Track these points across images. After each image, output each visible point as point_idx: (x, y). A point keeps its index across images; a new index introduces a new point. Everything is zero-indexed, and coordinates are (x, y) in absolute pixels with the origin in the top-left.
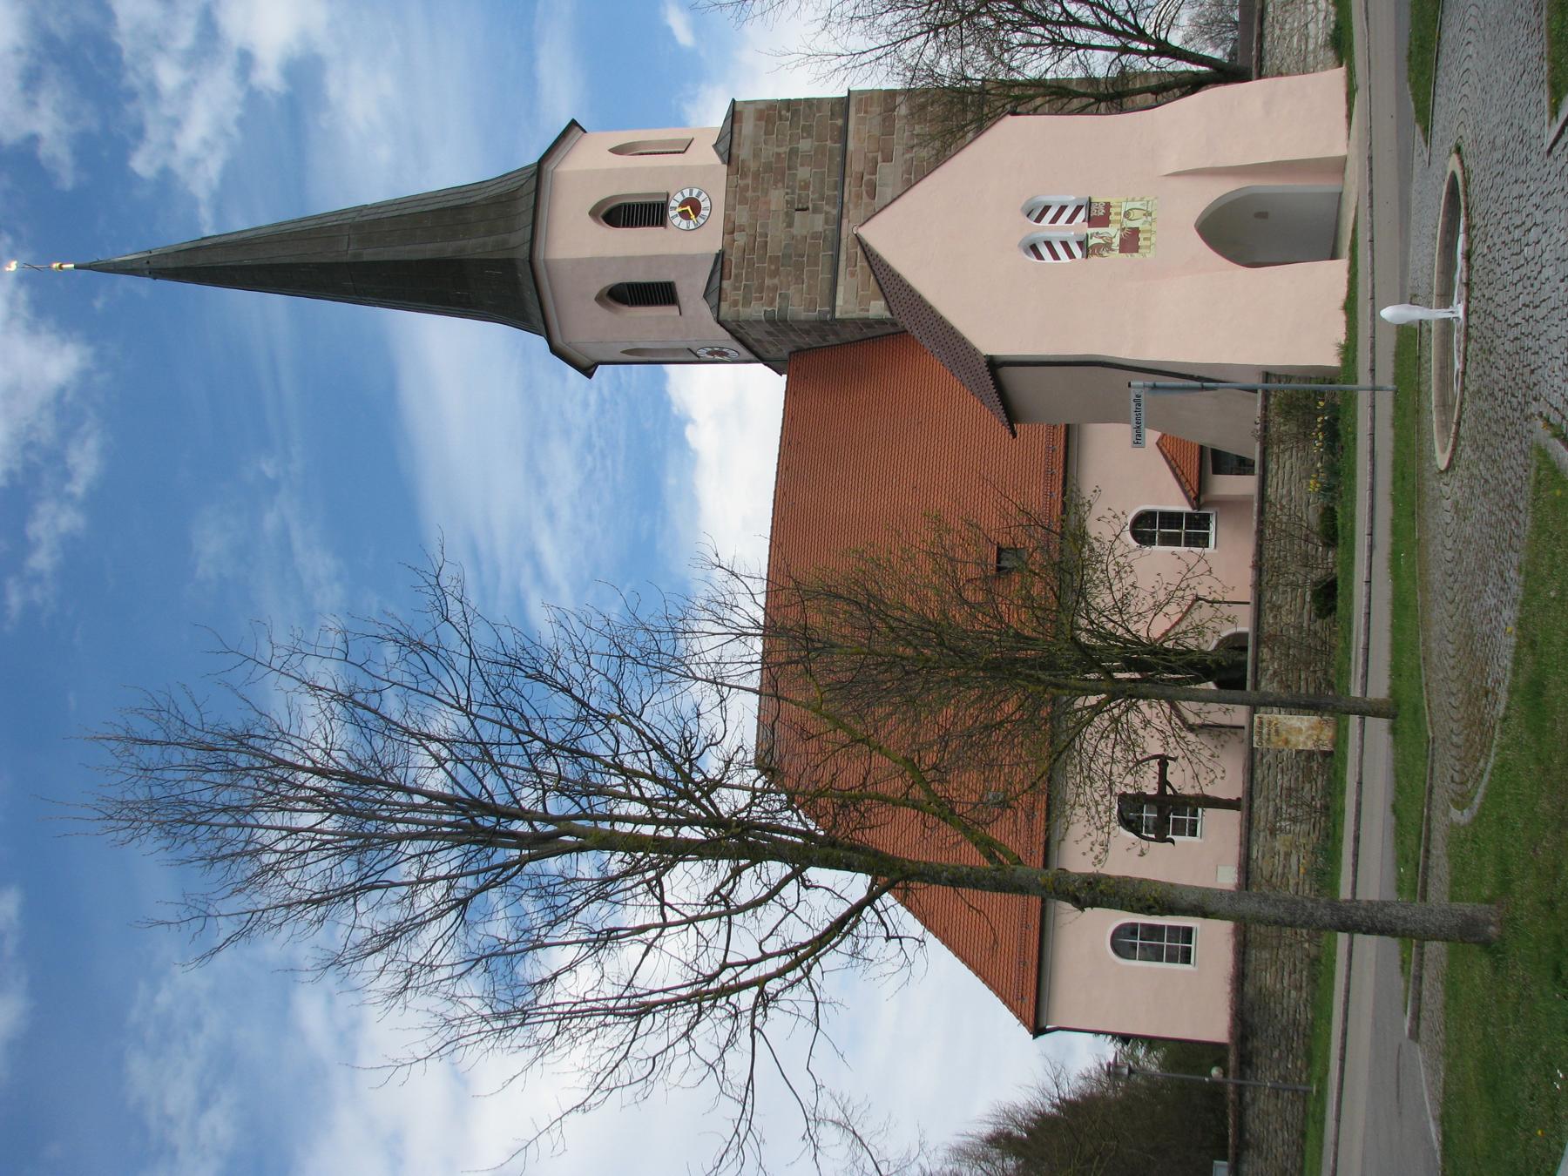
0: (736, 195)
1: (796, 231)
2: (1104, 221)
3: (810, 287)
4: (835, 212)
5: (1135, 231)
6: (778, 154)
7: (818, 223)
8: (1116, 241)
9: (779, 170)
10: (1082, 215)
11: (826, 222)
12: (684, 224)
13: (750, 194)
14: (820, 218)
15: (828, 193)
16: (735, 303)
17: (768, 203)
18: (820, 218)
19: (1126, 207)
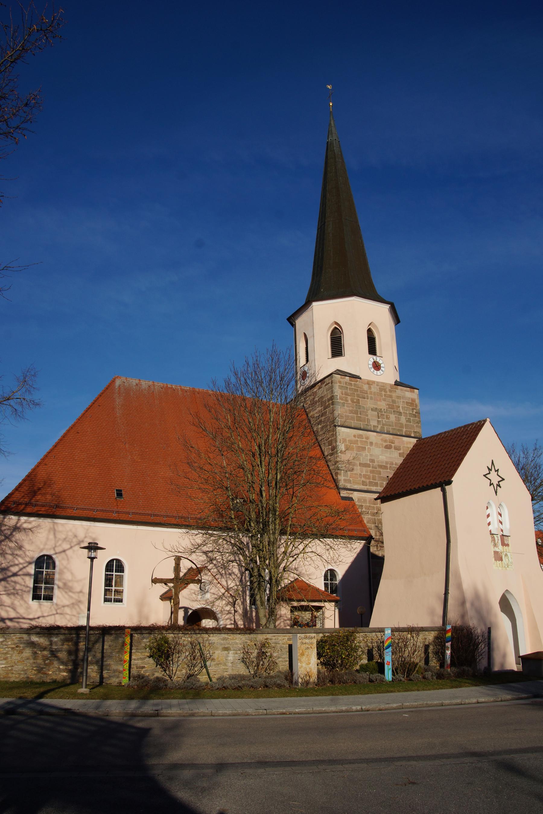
0: (382, 387)
1: (370, 412)
2: (503, 544)
3: (348, 416)
4: (378, 430)
6: (399, 407)
7: (373, 423)
8: (497, 550)
9: (393, 407)
11: (374, 426)
12: (371, 363)
13: (383, 393)
14: (375, 423)
15: (385, 427)
16: (340, 382)
17: (380, 400)
18: (375, 423)
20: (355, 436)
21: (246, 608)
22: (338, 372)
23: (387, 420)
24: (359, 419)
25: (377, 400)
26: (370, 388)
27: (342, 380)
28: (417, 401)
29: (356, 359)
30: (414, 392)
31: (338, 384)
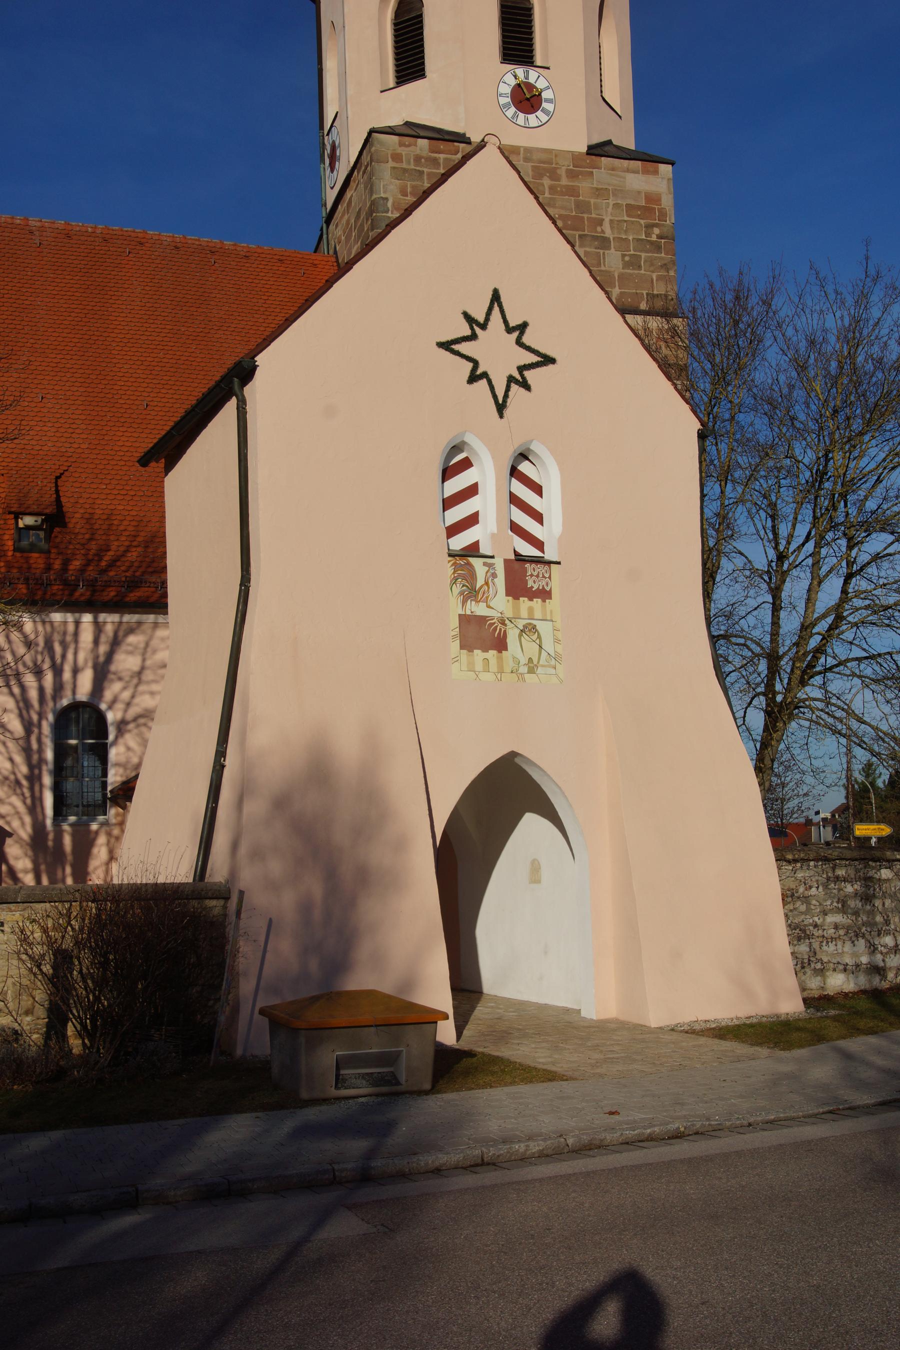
2: (517, 588)
5: (500, 644)
6: (600, 222)
8: (480, 610)
10: (527, 550)
12: (506, 89)
19: (544, 628)
21: (44, 826)
22: (412, 131)
27: (403, 151)
30: (656, 172)
31: (391, 164)
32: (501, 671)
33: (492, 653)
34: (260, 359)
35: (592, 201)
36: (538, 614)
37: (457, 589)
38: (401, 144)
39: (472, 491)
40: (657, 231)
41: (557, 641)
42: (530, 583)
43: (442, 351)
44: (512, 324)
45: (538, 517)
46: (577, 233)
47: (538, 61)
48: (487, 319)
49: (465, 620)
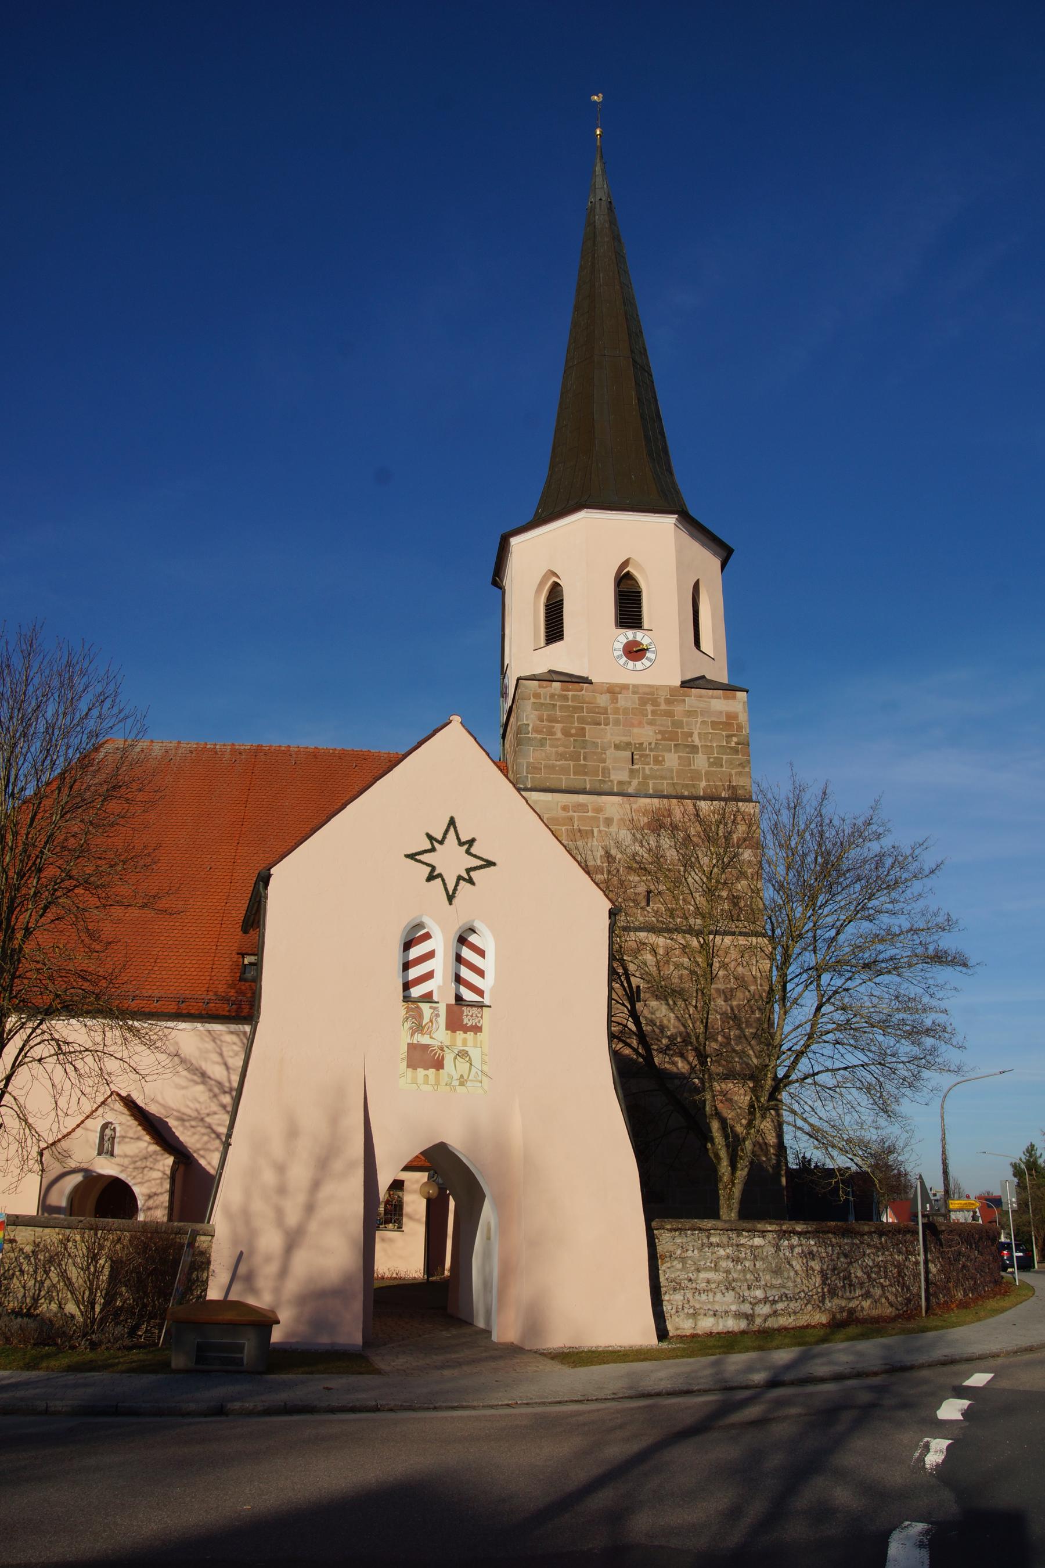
0: (648, 696)
1: (611, 752)
2: (454, 1024)
3: (553, 767)
4: (631, 790)
5: (439, 1065)
6: (691, 735)
7: (619, 775)
8: (425, 1040)
9: (675, 737)
11: (620, 783)
12: (619, 645)
13: (649, 708)
15: (651, 783)
17: (640, 725)
18: (624, 776)
19: (475, 1053)
20: (565, 808)
22: (552, 676)
23: (656, 767)
24: (581, 771)
25: (632, 725)
26: (615, 700)
27: (542, 691)
28: (743, 718)
29: (592, 646)
30: (734, 697)
31: (532, 700)
32: (438, 1083)
33: (432, 1071)
34: (272, 871)
35: (685, 720)
36: (470, 1042)
37: (407, 1025)
38: (540, 687)
39: (430, 955)
40: (735, 739)
41: (484, 1062)
42: (465, 1021)
43: (409, 860)
44: (463, 840)
45: (481, 973)
46: (673, 743)
47: (646, 625)
48: (444, 838)
49: (411, 1047)
